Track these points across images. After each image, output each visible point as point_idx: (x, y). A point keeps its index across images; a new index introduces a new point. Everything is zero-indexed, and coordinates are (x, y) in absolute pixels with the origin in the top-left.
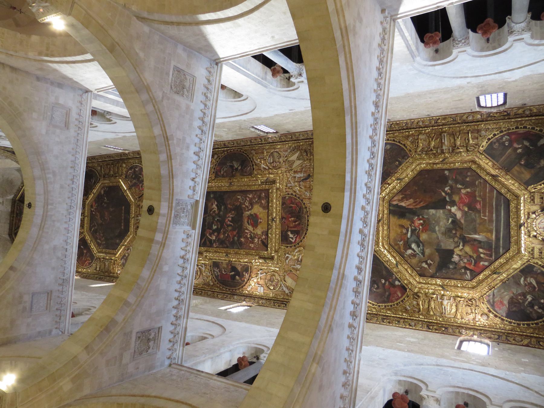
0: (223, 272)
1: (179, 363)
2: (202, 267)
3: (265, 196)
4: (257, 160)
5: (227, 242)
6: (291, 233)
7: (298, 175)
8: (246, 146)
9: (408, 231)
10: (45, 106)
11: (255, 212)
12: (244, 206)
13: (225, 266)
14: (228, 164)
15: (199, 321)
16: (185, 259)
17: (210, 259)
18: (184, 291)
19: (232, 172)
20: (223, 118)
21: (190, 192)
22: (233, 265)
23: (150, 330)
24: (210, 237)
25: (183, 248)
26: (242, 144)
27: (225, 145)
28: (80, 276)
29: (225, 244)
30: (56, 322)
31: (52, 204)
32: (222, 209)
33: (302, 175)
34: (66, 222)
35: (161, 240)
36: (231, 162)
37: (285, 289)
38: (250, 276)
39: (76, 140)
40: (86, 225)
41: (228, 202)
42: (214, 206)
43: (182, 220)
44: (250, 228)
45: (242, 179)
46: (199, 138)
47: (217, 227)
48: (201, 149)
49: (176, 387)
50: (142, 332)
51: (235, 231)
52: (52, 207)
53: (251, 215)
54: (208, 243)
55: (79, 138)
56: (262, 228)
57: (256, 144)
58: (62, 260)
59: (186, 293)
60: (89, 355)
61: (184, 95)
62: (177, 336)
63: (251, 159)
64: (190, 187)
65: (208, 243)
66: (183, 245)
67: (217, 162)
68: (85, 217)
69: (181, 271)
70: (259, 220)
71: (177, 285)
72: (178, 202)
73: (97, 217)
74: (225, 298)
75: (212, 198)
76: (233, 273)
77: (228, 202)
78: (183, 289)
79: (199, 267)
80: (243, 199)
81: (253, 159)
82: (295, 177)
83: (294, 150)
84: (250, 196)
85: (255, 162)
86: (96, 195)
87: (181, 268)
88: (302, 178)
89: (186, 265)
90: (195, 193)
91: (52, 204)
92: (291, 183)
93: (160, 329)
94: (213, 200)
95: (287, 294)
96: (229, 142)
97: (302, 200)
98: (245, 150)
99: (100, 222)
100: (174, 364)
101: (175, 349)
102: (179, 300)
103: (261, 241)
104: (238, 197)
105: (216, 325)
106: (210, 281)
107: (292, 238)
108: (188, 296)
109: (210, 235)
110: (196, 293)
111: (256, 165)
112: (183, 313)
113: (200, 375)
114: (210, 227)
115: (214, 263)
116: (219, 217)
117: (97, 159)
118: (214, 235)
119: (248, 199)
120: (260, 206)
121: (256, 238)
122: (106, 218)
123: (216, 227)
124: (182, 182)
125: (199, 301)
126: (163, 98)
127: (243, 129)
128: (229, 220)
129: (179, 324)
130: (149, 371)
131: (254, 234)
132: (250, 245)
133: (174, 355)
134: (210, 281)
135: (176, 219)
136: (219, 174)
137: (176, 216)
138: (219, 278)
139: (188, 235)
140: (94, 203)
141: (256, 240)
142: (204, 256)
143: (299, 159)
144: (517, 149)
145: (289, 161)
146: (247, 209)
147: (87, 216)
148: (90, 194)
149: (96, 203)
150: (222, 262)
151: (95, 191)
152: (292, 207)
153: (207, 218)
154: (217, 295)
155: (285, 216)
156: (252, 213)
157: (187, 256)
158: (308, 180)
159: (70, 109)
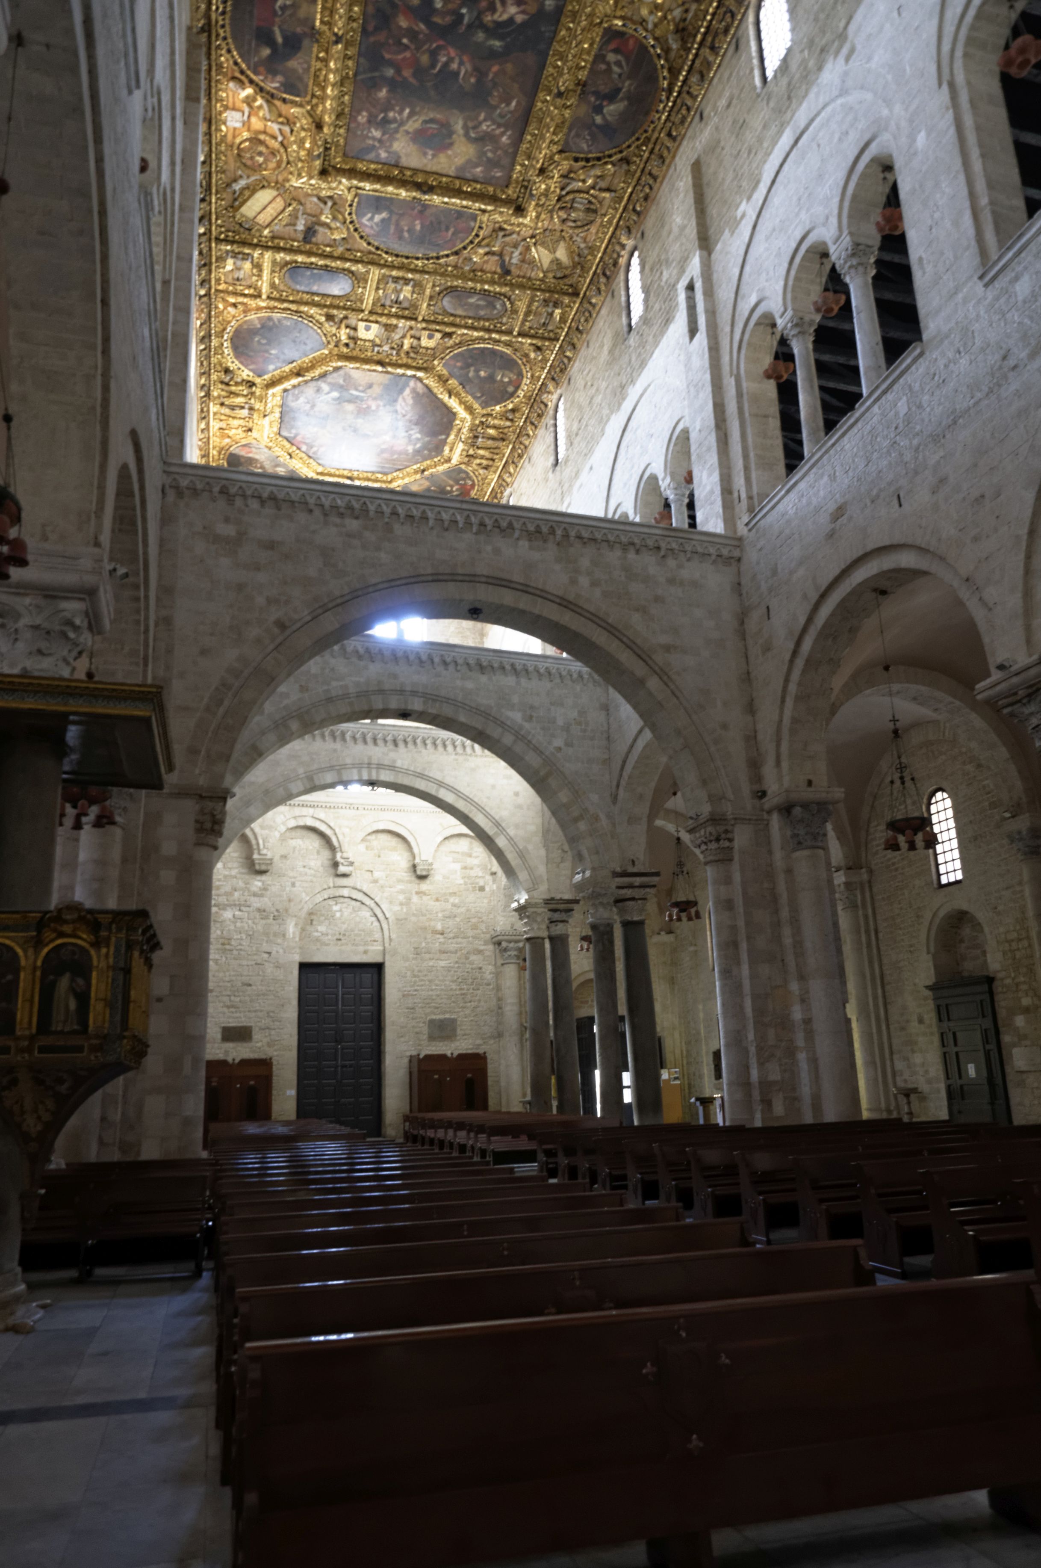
3: (494, 177)
5: (381, 37)
6: (383, 220)
7: (516, 254)
9: (363, 391)
11: (456, 146)
12: (482, 116)
14: (627, 83)
22: (306, 42)
29: (377, 29)
33: (514, 261)
36: (629, 97)
37: (242, 183)
38: (272, 96)
42: (513, 10)
44: (413, 125)
51: (414, 75)
53: (451, 133)
56: (407, 155)
70: (430, 152)
76: (280, 40)
77: (509, 67)
81: (606, 163)
82: (515, 246)
83: (579, 255)
84: (504, 139)
88: (507, 259)
92: (504, 236)
95: (228, 185)
97: (456, 253)
103: (374, 146)
104: (514, 103)
107: (371, 219)
111: (584, 167)
116: (470, 26)
119: (498, 132)
120: (469, 161)
121: (383, 134)
128: (451, 60)
131: (396, 131)
136: (612, 46)
141: (376, 133)
143: (552, 262)
144: (452, 487)
145: (558, 241)
146: (470, 124)
152: (447, 229)
155: (428, 212)
156: (454, 136)
158: (499, 270)
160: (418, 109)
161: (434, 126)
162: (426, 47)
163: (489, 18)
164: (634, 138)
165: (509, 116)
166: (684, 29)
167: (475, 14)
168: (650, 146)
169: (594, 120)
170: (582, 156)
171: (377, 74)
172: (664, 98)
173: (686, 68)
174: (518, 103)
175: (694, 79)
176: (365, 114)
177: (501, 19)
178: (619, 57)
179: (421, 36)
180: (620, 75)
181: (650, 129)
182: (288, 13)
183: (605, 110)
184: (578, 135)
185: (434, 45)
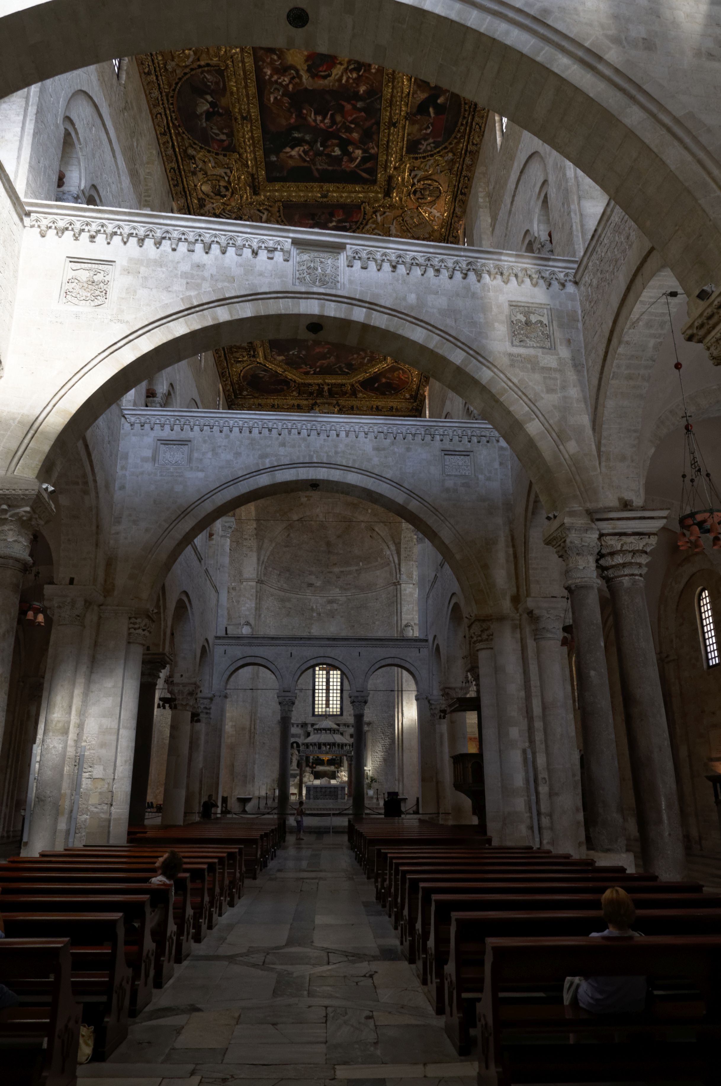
0: (429, 131)
1: (575, 266)
2: (416, 176)
4: (188, 57)
8: (159, 85)
10: (161, 476)
12: (291, 87)
13: (417, 127)
15: (516, 198)
16: (398, 263)
17: (401, 160)
18: (452, 261)
19: (220, 115)
20: (114, 156)
21: (279, 256)
23: (512, 322)
24: (358, 161)
25: (379, 268)
26: (156, 93)
27: (164, 134)
28: (425, 387)
30: (488, 442)
31: (311, 457)
32: (299, 135)
34: (338, 435)
35: (364, 310)
39: (205, 428)
40: (339, 381)
41: (284, 122)
42: (294, 153)
43: (328, 271)
44: (337, 71)
45: (232, 93)
46: (177, 245)
47: (337, 145)
48: (197, 240)
49: (609, 283)
50: (513, 336)
51: (343, 107)
52: (315, 456)
53: (309, 70)
54: (368, 165)
55: (202, 424)
57: (153, 61)
58: (395, 438)
59: (456, 258)
60: (534, 419)
61: (106, 279)
62: (529, 272)
63: (187, 70)
64: (269, 258)
65: (368, 165)
66: (372, 266)
67: (201, 148)
68: (325, 382)
69: (418, 268)
71: (441, 276)
72: (297, 280)
73: (325, 365)
74: (480, 128)
75: (277, 157)
76: (431, 110)
77: (284, 122)
78: (450, 265)
79: (416, 181)
80: (276, 89)
81: (186, 67)
84: (269, 72)
85: (192, 62)
86: (285, 367)
87: (413, 267)
89: (408, 259)
90: (279, 247)
91: (311, 457)
93: (513, 305)
94: (282, 155)
96: (156, 125)
98: (170, 85)
99: (332, 359)
100: (575, 277)
101: (550, 274)
102: (469, 270)
104: (272, 99)
105: (527, 168)
106: (446, 158)
108: (462, 254)
109: (352, 160)
110: (466, 188)
112: (491, 262)
113: (600, 236)
114: (337, 160)
115: (408, 151)
116: (316, 142)
117: (224, 369)
118: (353, 152)
119: (275, 77)
122: (326, 350)
123: (337, 149)
124: (261, 274)
125: (480, 189)
126: (120, 321)
127: (127, 102)
128: (322, 121)
129: (508, 268)
130: (578, 321)
132: (373, 71)
133: (561, 276)
134: (446, 158)
135: (328, 283)
136: (226, 143)
137: (323, 283)
138: (439, 139)
139: (354, 258)
140: (301, 370)
142: (395, 173)
146: (297, 80)
147: (324, 380)
148: (286, 377)
149: (301, 368)
150: (409, 134)
151: (279, 370)
153: (320, 167)
154: (473, 144)
156: (306, 68)
157: (393, 258)
159: (158, 440)
160: (337, 84)
161: (322, 74)
162: (339, 126)
163: (306, 147)
164: (177, 90)
165: (272, 90)
166: (191, 159)
167: (314, 148)
168: (164, 94)
169: (212, 97)
170: (206, 69)
171: (368, 101)
172: (176, 122)
173: (176, 144)
174: (270, 100)
175: (170, 152)
176: (373, 71)
177: (299, 148)
178: (218, 138)
179: (343, 131)
180: (212, 128)
181: (170, 99)
182: (425, 126)
183: (208, 105)
184: (217, 83)
185: (334, 127)
